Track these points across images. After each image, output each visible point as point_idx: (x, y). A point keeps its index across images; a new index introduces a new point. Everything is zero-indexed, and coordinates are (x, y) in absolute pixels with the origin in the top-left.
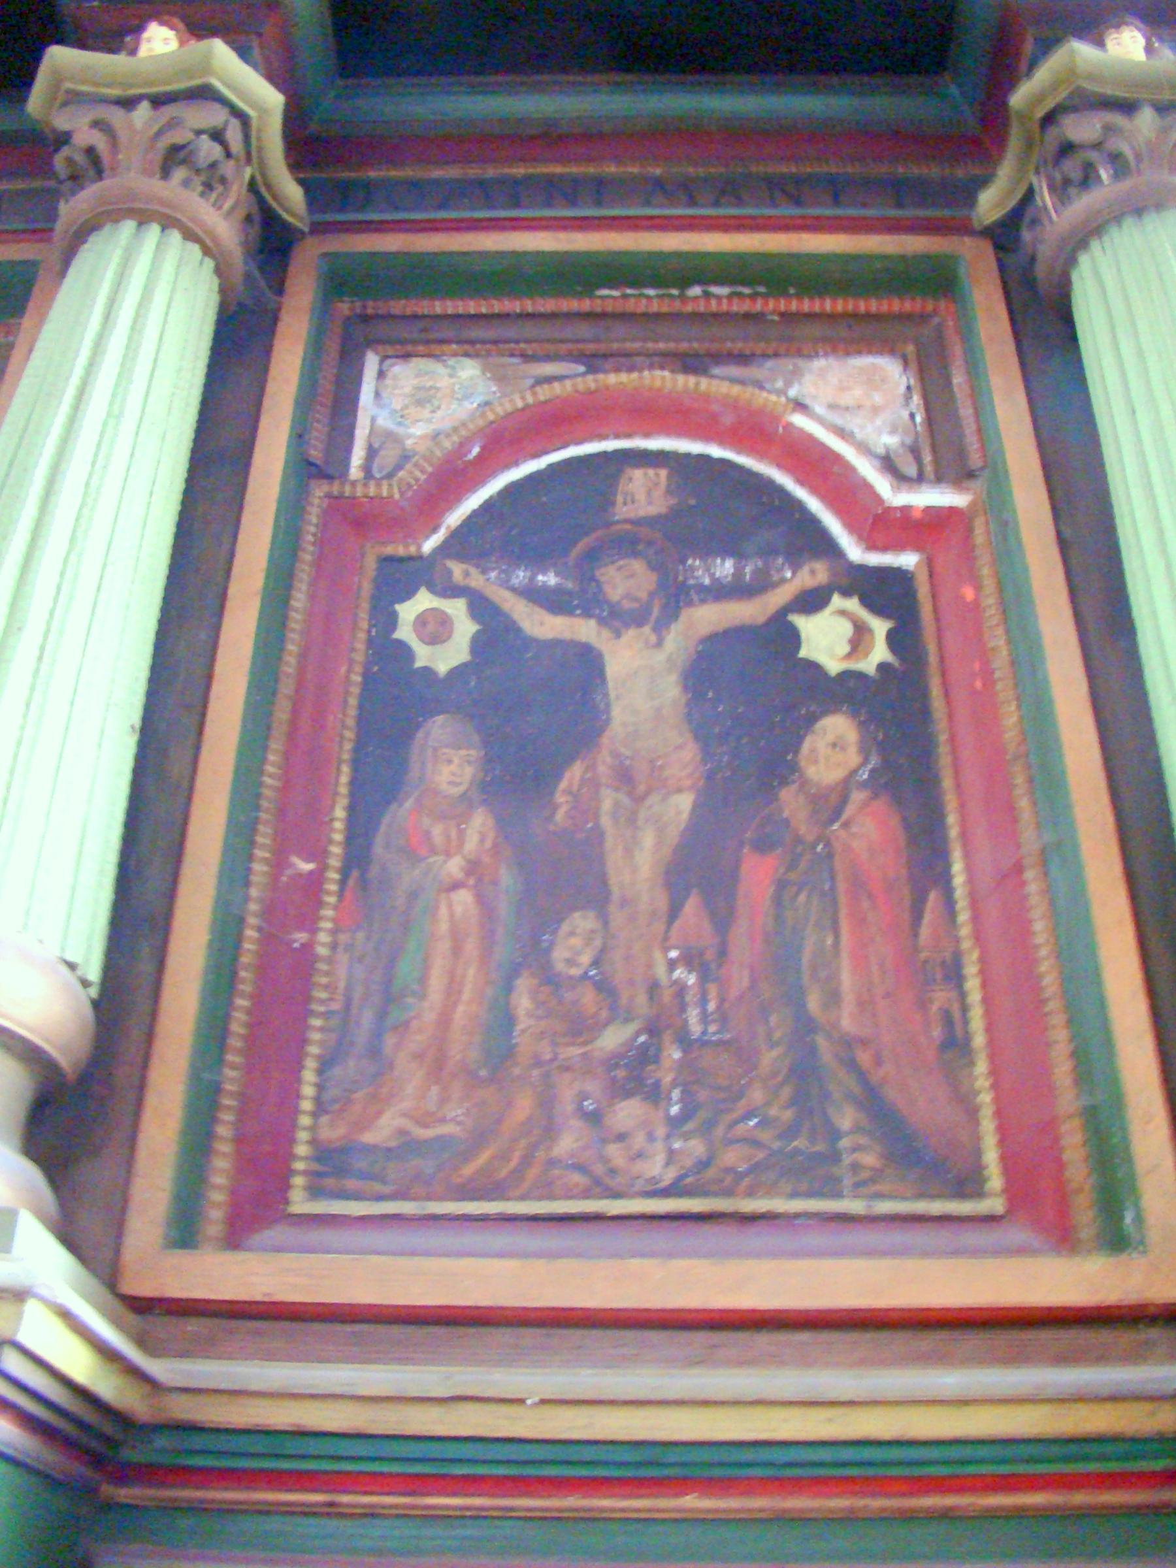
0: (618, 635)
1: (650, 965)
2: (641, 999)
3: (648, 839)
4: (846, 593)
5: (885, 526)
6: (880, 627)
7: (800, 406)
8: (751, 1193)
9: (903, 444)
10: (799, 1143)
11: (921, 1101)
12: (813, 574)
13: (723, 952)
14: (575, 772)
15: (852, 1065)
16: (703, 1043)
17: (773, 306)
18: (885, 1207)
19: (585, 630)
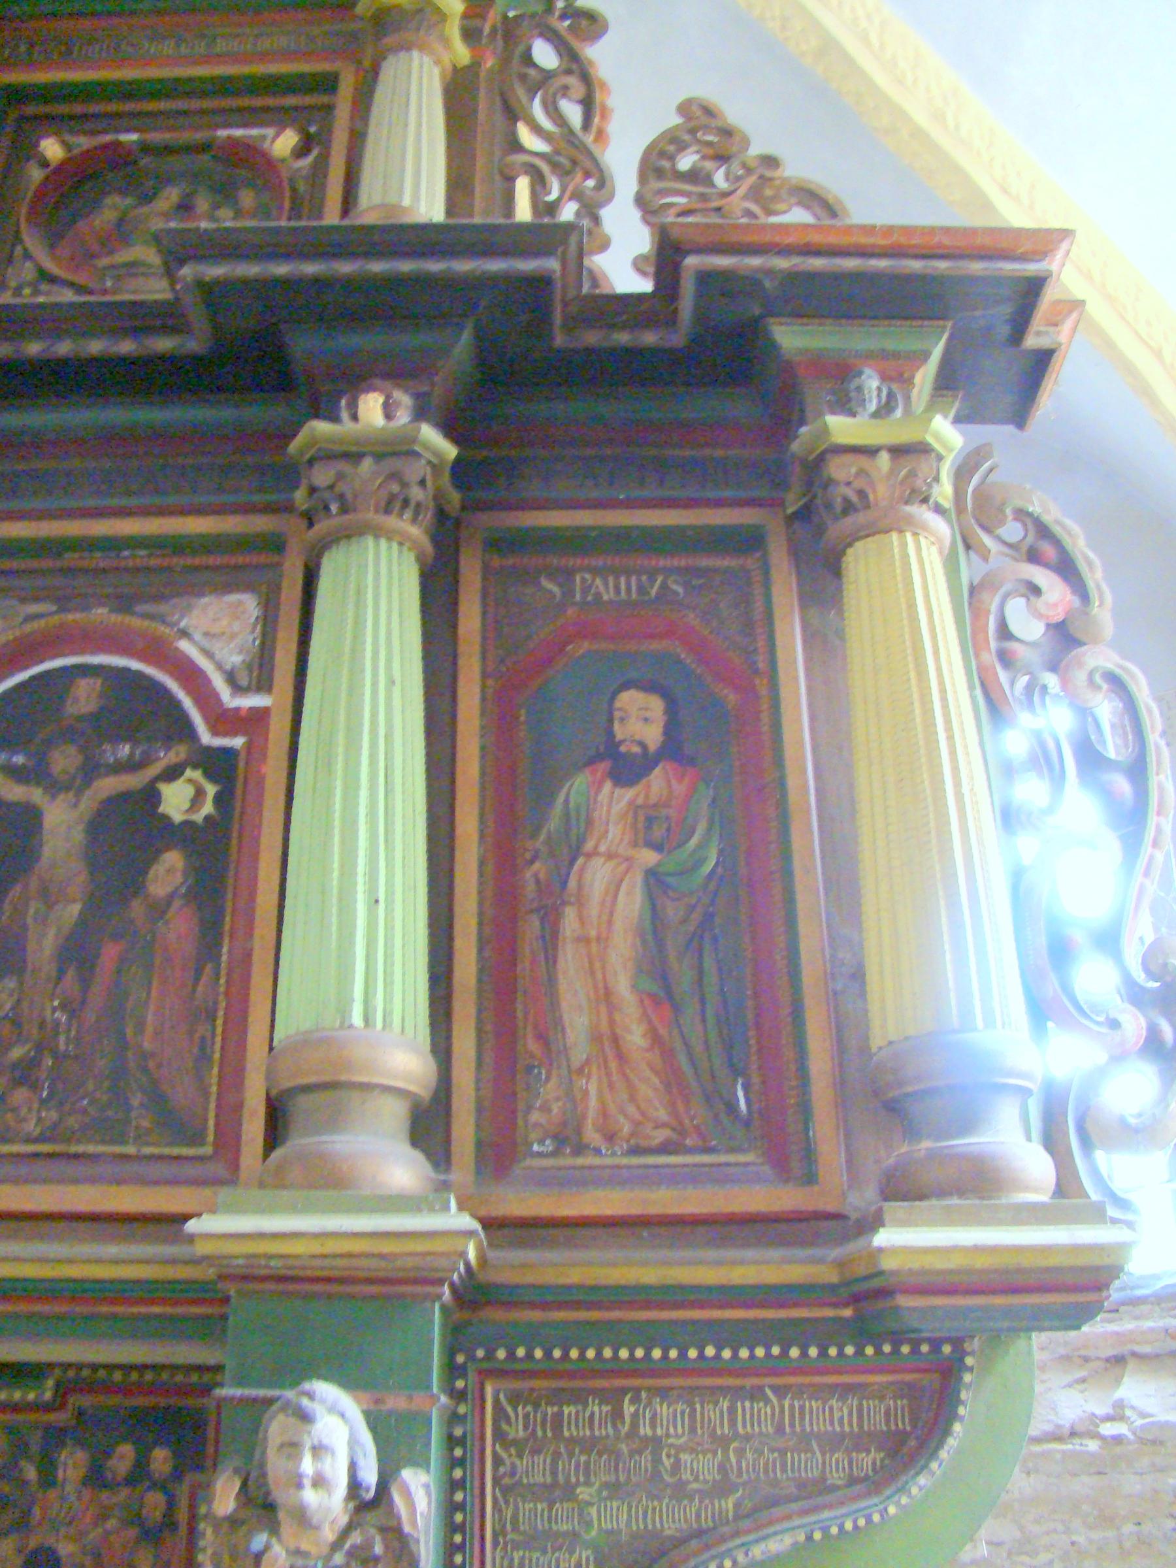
0: (54, 797)
1: (43, 1009)
2: (35, 1031)
3: (52, 932)
4: (195, 767)
5: (224, 720)
6: (211, 790)
7: (184, 634)
8: (79, 1141)
9: (244, 661)
10: (110, 1113)
11: (181, 1092)
12: (178, 753)
13: (83, 1002)
14: (16, 891)
15: (144, 1069)
16: (66, 1056)
17: (178, 562)
18: (148, 1150)
19: (36, 795)
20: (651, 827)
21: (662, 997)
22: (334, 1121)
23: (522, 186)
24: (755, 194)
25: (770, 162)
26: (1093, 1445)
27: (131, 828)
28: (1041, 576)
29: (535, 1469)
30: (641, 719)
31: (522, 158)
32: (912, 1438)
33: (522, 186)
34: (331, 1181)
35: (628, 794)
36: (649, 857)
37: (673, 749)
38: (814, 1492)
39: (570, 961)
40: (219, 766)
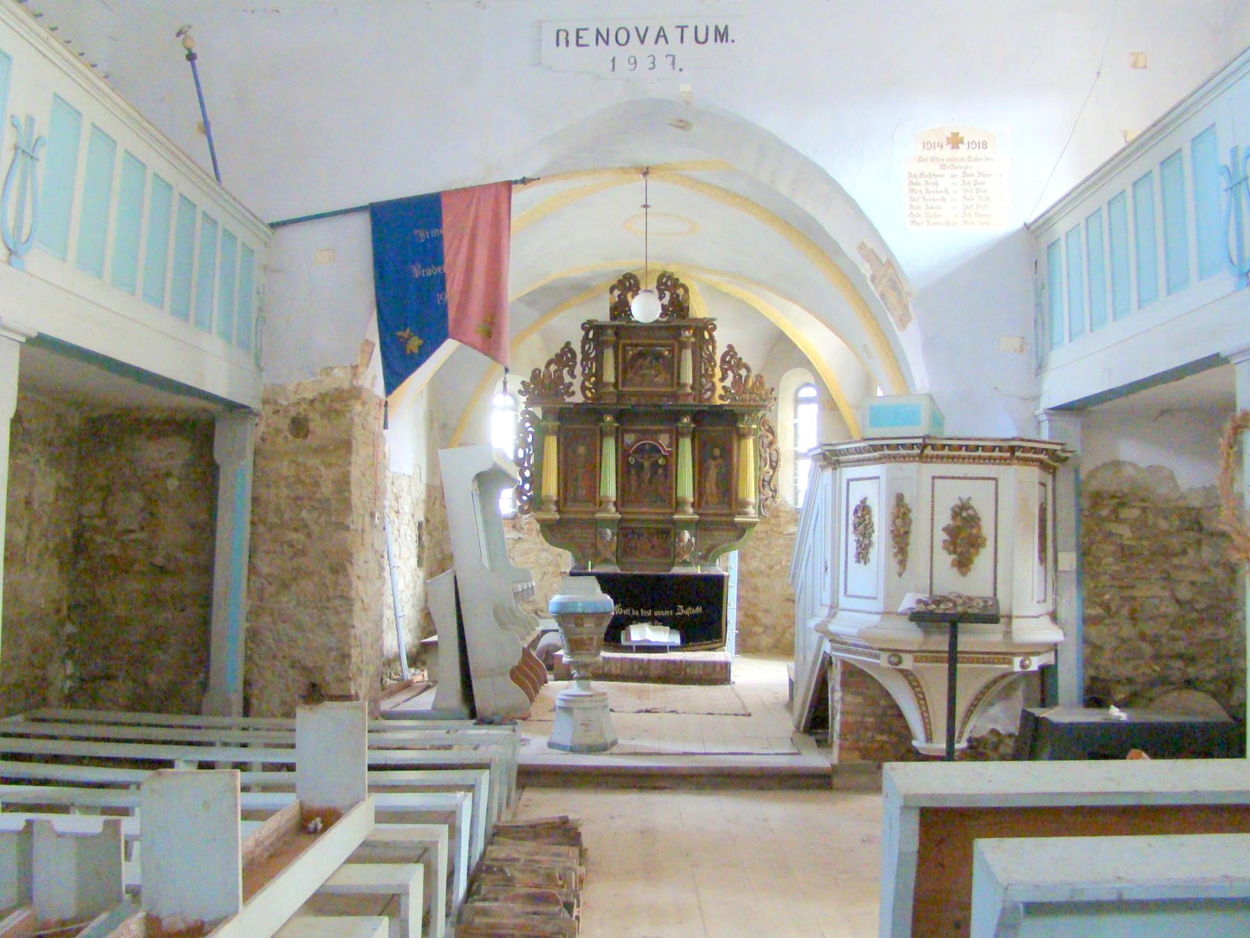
20: (716, 466)
21: (718, 487)
27: (655, 465)
30: (717, 452)
32: (740, 537)
34: (685, 512)
37: (721, 456)
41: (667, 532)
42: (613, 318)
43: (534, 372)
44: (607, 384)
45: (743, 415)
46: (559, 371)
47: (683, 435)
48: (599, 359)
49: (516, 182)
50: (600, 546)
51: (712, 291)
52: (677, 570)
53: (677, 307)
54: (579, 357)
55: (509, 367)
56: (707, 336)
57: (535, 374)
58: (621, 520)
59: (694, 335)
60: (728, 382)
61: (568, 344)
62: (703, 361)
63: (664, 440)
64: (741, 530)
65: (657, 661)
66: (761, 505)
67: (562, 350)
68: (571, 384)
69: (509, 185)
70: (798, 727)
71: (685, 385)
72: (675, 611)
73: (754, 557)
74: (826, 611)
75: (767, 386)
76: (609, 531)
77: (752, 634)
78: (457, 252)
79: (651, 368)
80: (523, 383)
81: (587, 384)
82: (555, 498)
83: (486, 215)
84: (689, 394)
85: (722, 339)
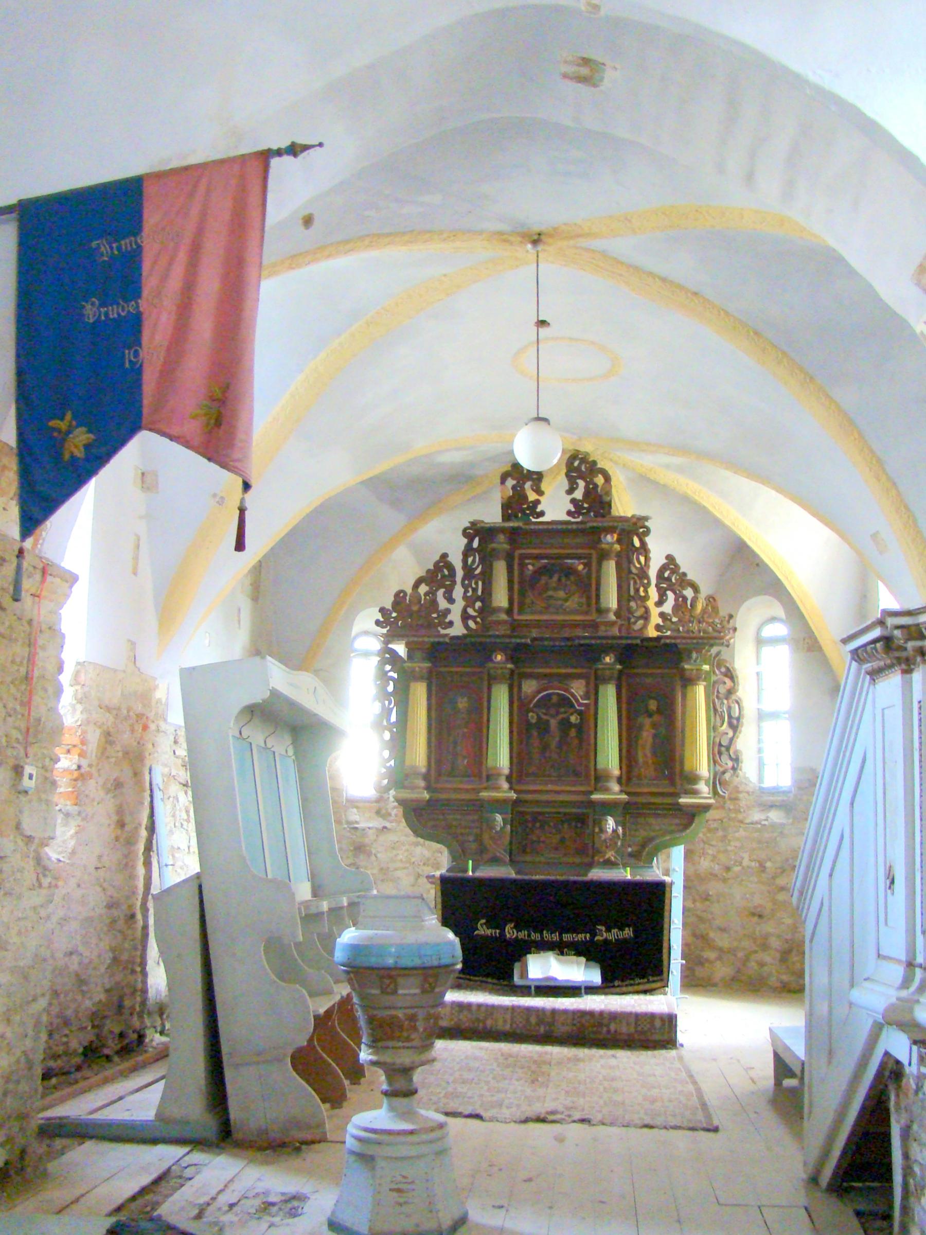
5: (580, 705)
12: (572, 710)
20: (654, 726)
22: (607, 781)
23: (632, 583)
24: (680, 585)
25: (684, 574)
26: (759, 826)
27: (565, 725)
28: (727, 680)
29: (633, 827)
30: (653, 705)
31: (632, 576)
32: (686, 826)
33: (632, 583)
34: (607, 790)
35: (651, 720)
36: (653, 731)
37: (659, 711)
38: (671, 832)
39: (639, 748)
40: (580, 713)
41: (584, 818)
42: (506, 517)
43: (397, 595)
44: (499, 609)
45: (689, 652)
46: (432, 593)
47: (606, 681)
48: (487, 578)
49: (279, 153)
50: (486, 836)
51: (644, 481)
52: (598, 874)
53: (596, 503)
54: (460, 574)
55: (253, 482)
56: (637, 543)
57: (399, 597)
58: (516, 802)
59: (619, 541)
60: (668, 607)
61: (444, 556)
62: (632, 578)
63: (578, 689)
64: (690, 816)
65: (565, 1012)
66: (717, 781)
67: (436, 564)
68: (448, 611)
69: (265, 156)
70: (814, 1180)
71: (608, 610)
72: (594, 935)
73: (704, 854)
74: (897, 972)
75: (723, 612)
76: (499, 818)
77: (701, 962)
78: (164, 279)
79: (555, 589)
80: (382, 610)
81: (471, 611)
82: (424, 770)
83: (222, 207)
84: (613, 624)
85: (658, 550)
